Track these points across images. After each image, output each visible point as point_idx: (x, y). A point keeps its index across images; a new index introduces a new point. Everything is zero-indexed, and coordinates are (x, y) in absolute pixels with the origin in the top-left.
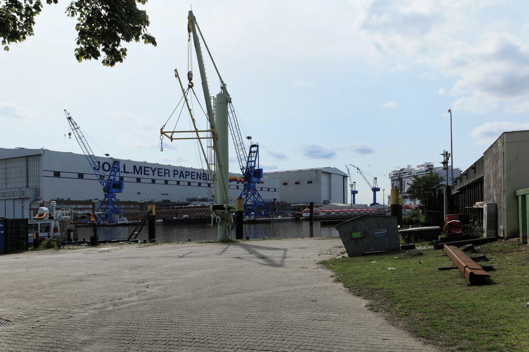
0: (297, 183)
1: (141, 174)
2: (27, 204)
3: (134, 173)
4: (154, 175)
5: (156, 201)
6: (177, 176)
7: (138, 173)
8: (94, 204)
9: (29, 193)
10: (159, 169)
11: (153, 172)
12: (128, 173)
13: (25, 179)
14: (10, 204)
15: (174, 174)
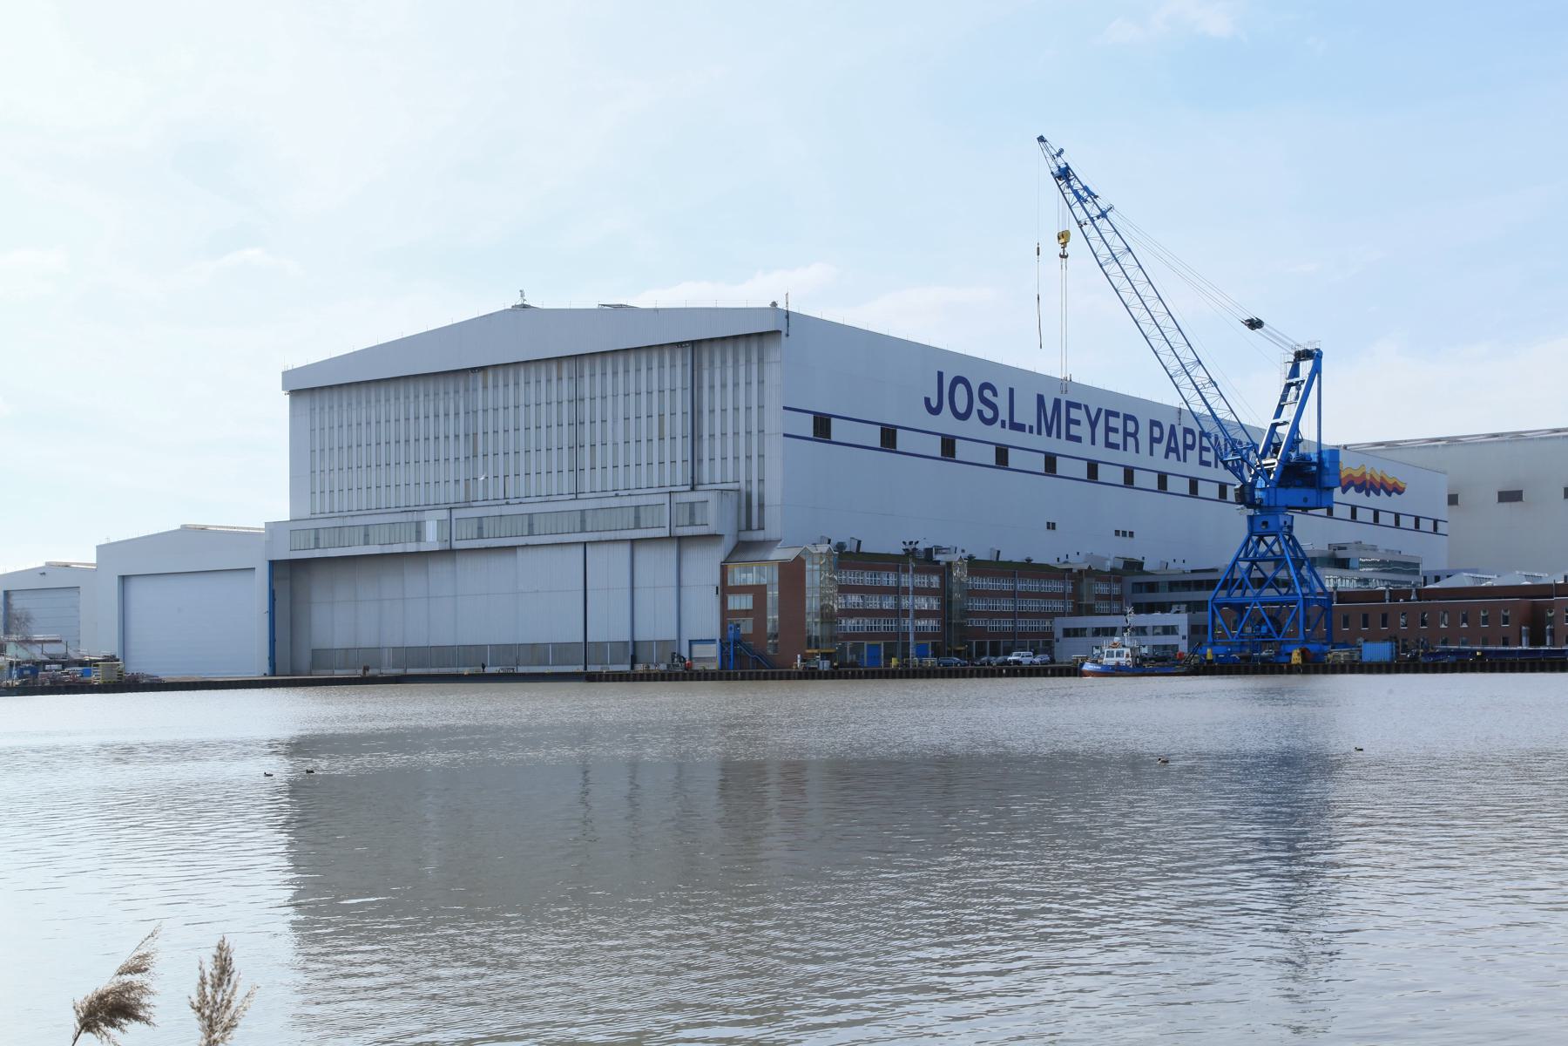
0: (1510, 496)
1: (1059, 436)
2: (704, 567)
3: (1039, 433)
4: (1093, 443)
5: (1108, 566)
6: (1160, 449)
7: (1049, 434)
8: (946, 571)
9: (715, 516)
10: (1109, 413)
11: (1093, 424)
12: (1021, 428)
13: (681, 449)
14: (610, 565)
15: (1153, 440)
